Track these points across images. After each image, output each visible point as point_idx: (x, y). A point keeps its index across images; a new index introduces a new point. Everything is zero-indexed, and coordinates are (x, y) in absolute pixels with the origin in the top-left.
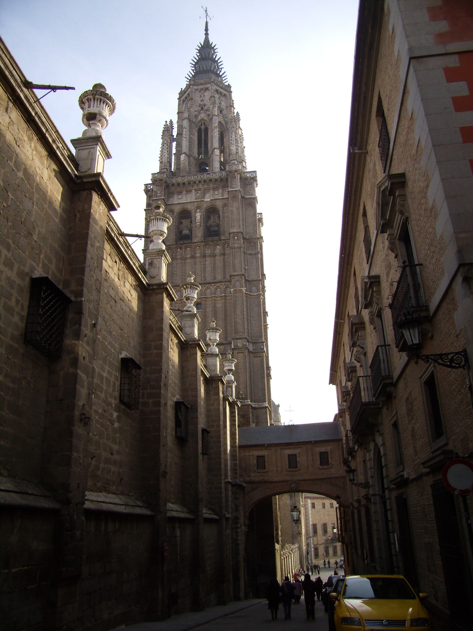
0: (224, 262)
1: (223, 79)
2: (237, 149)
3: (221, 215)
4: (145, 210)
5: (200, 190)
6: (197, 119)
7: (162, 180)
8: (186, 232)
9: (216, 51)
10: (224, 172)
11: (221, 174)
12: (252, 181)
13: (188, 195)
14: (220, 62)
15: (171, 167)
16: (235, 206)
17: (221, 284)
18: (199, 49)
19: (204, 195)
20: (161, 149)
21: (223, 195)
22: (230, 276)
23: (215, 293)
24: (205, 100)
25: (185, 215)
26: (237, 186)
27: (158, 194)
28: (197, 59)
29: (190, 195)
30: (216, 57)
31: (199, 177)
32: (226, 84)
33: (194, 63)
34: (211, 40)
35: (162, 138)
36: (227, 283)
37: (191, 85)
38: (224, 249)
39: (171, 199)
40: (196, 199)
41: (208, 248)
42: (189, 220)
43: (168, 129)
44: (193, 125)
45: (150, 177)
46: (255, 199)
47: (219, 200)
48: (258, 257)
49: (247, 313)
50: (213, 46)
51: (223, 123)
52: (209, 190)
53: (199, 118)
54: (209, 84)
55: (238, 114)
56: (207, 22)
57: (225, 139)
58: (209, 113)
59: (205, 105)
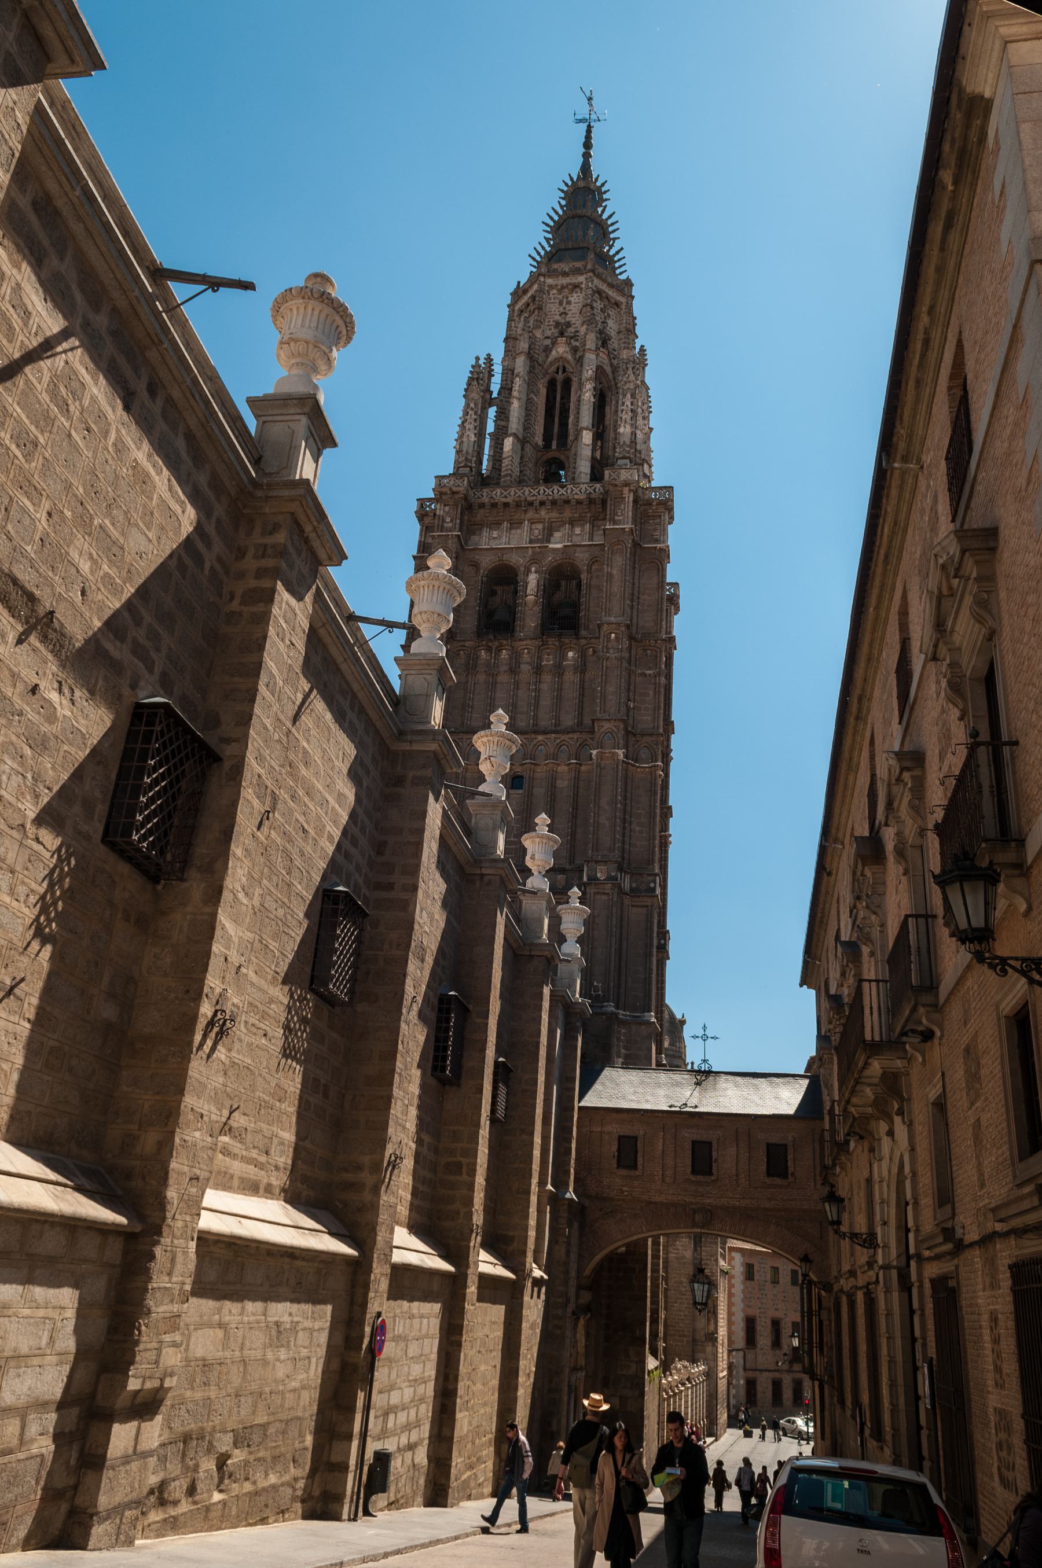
0: (582, 688)
1: (617, 265)
2: (634, 434)
4: (414, 557)
5: (540, 521)
6: (547, 357)
7: (458, 493)
9: (605, 196)
10: (598, 486)
11: (590, 490)
12: (661, 509)
13: (513, 531)
14: (613, 224)
15: (481, 463)
17: (570, 735)
18: (565, 189)
19: (551, 535)
20: (460, 422)
21: (591, 539)
27: (445, 525)
28: (561, 212)
29: (519, 531)
30: (603, 212)
31: (542, 492)
32: (623, 277)
33: (552, 224)
36: (584, 736)
37: (540, 275)
38: (583, 655)
39: (475, 538)
40: (531, 542)
43: (479, 376)
45: (432, 483)
47: (583, 549)
49: (625, 805)
50: (598, 184)
51: (608, 369)
52: (563, 523)
55: (642, 349)
57: (607, 408)
58: (577, 344)
59: (568, 324)
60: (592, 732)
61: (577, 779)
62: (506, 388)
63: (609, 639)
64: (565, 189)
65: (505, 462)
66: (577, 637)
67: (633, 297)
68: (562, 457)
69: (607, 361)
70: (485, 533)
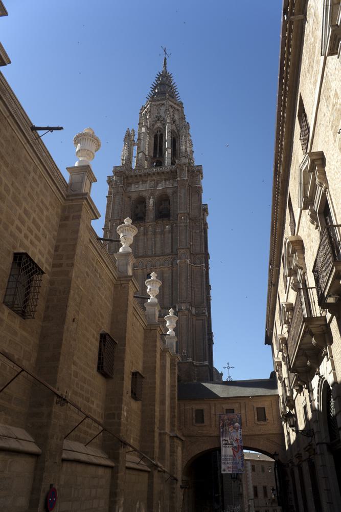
0: (172, 239)
3: (171, 200)
4: (107, 197)
10: (174, 166)
12: (198, 173)
16: (182, 193)
19: (158, 185)
25: (142, 201)
29: (145, 185)
33: (153, 87)
39: (129, 188)
43: (128, 136)
51: (176, 131)
52: (162, 180)
56: (165, 58)
59: (161, 116)
63: (181, 219)
67: (183, 108)
68: (161, 160)
69: (175, 128)
70: (133, 186)
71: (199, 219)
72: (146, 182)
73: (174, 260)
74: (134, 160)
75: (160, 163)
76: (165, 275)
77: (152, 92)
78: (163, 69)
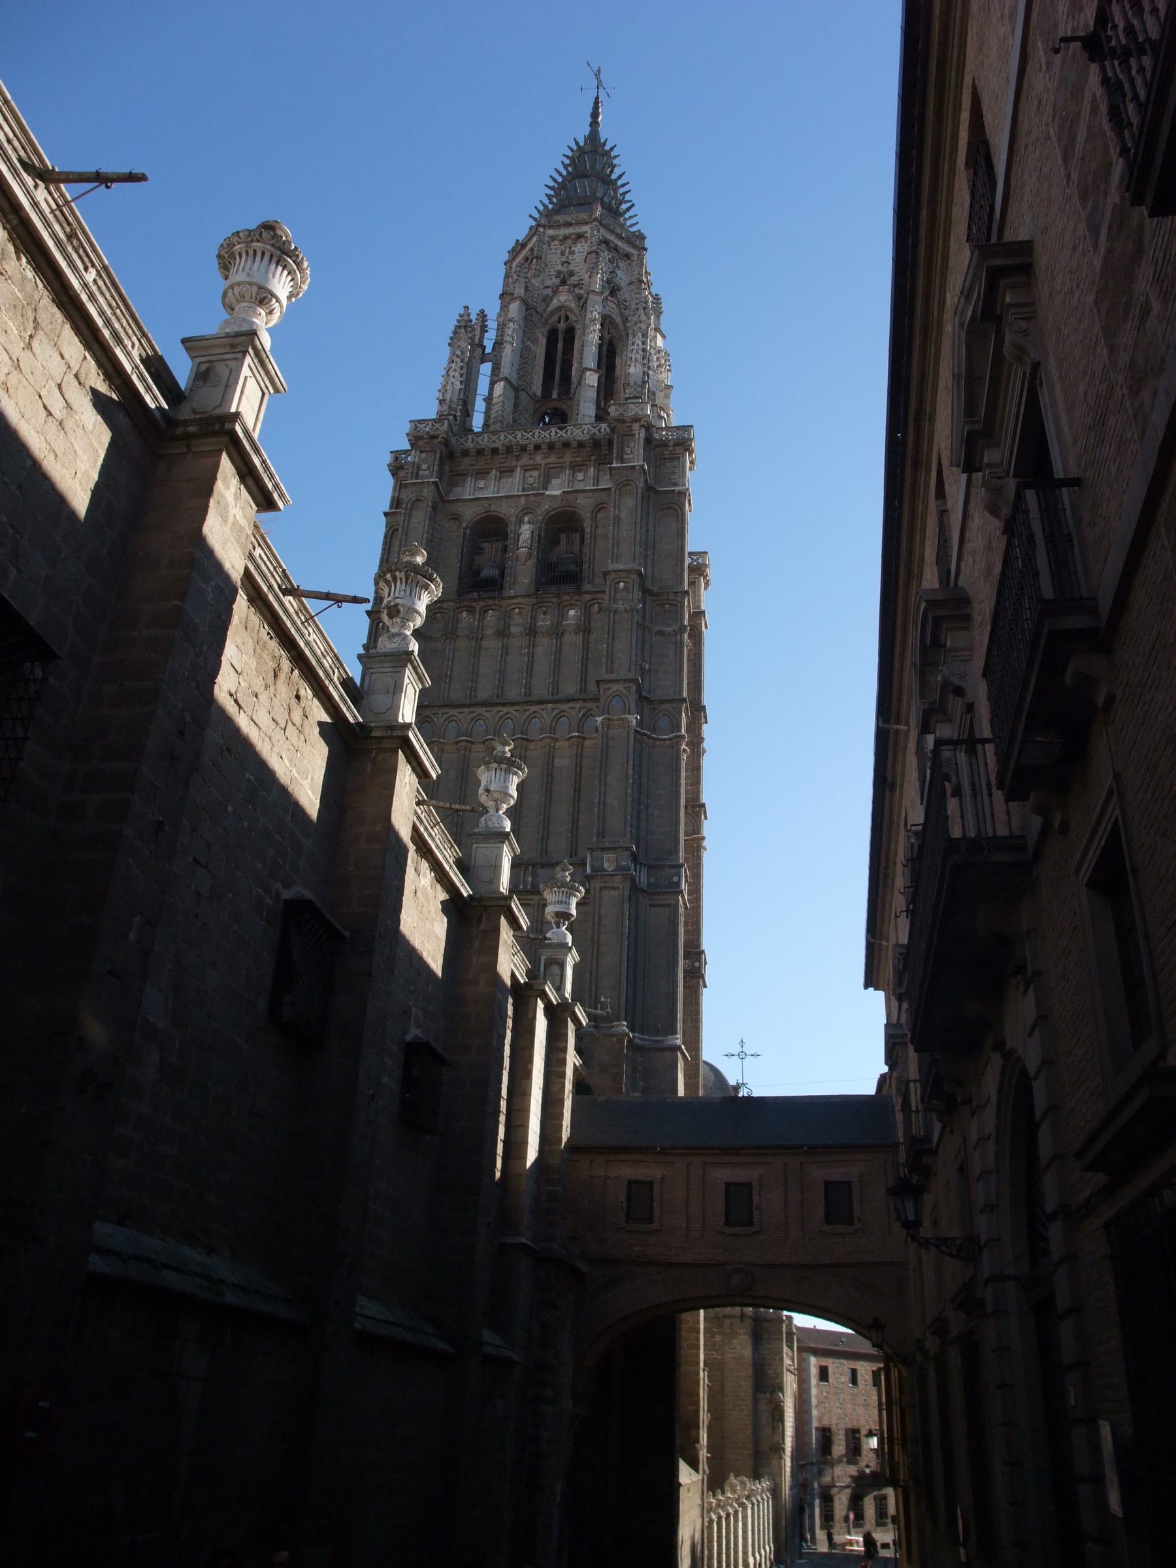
4: (386, 514)
6: (547, 306)
7: (436, 437)
8: (489, 572)
10: (604, 426)
12: (679, 450)
13: (503, 480)
14: (623, 186)
17: (571, 705)
21: (597, 481)
22: (598, 682)
23: (553, 730)
24: (573, 263)
25: (492, 529)
26: (636, 456)
28: (565, 173)
29: (510, 480)
31: (537, 434)
34: (604, 133)
35: (450, 345)
36: (589, 705)
38: (587, 613)
39: (458, 489)
41: (545, 614)
42: (500, 545)
43: (468, 329)
44: (536, 318)
45: (407, 428)
46: (683, 494)
48: (682, 642)
50: (607, 148)
51: (618, 319)
53: (555, 303)
54: (587, 223)
56: (597, 98)
59: (572, 274)
60: (597, 700)
61: (579, 757)
62: (498, 344)
63: (616, 590)
64: (570, 154)
65: (496, 408)
66: (580, 592)
67: (646, 249)
68: (564, 407)
70: (469, 483)
71: (676, 593)
72: (512, 471)
73: (588, 715)
74: (480, 405)
75: (561, 417)
76: (558, 762)
77: (551, 202)
78: (587, 130)
